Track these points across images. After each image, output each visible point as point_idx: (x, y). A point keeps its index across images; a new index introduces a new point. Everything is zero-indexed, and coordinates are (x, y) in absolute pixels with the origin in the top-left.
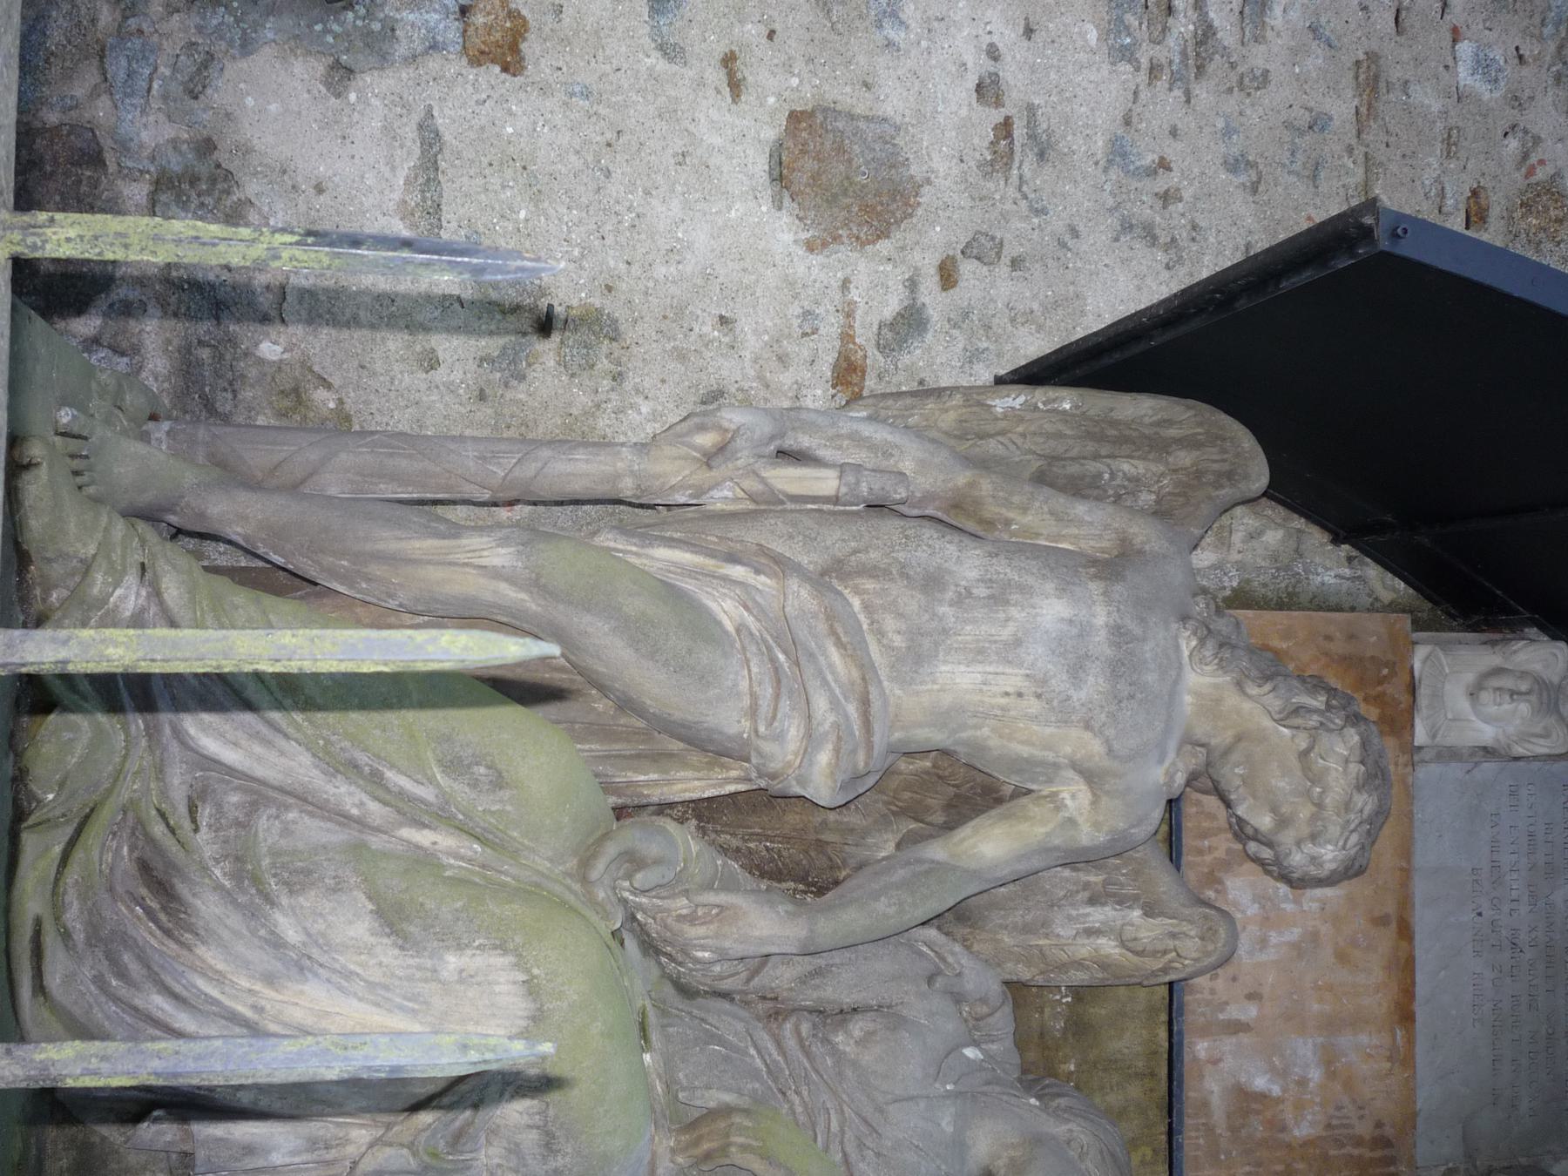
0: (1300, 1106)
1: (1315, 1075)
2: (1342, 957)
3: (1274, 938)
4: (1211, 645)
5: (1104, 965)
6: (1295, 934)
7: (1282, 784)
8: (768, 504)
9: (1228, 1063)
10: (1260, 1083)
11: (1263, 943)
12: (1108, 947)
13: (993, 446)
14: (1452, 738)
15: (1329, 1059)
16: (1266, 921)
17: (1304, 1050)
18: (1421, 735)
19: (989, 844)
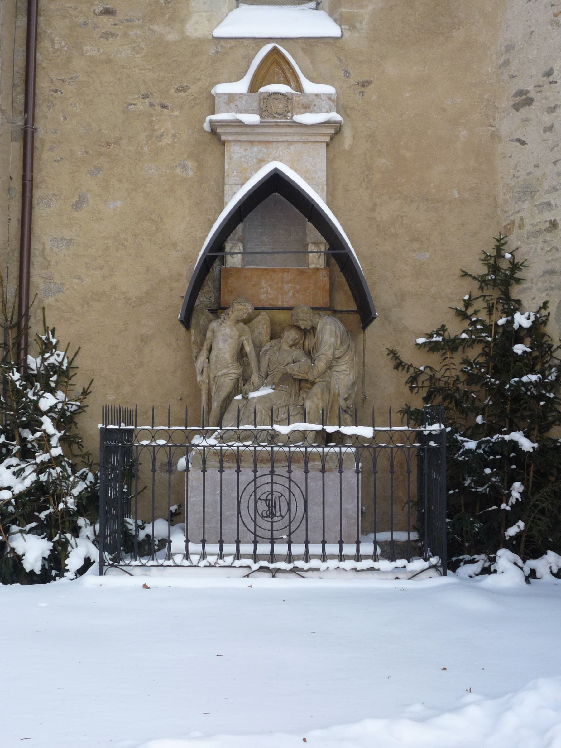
0: (294, 288)
1: (290, 285)
2: (273, 280)
3: (269, 292)
4: (225, 321)
5: (266, 328)
6: (269, 288)
7: (241, 313)
8: (209, 377)
9: (288, 300)
10: (291, 294)
11: (270, 293)
12: (265, 326)
13: (199, 340)
14: (240, 261)
15: (288, 283)
16: (267, 293)
17: (287, 287)
18: (240, 266)
19: (248, 349)
